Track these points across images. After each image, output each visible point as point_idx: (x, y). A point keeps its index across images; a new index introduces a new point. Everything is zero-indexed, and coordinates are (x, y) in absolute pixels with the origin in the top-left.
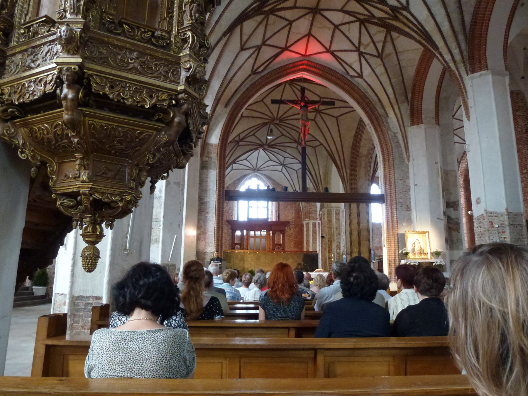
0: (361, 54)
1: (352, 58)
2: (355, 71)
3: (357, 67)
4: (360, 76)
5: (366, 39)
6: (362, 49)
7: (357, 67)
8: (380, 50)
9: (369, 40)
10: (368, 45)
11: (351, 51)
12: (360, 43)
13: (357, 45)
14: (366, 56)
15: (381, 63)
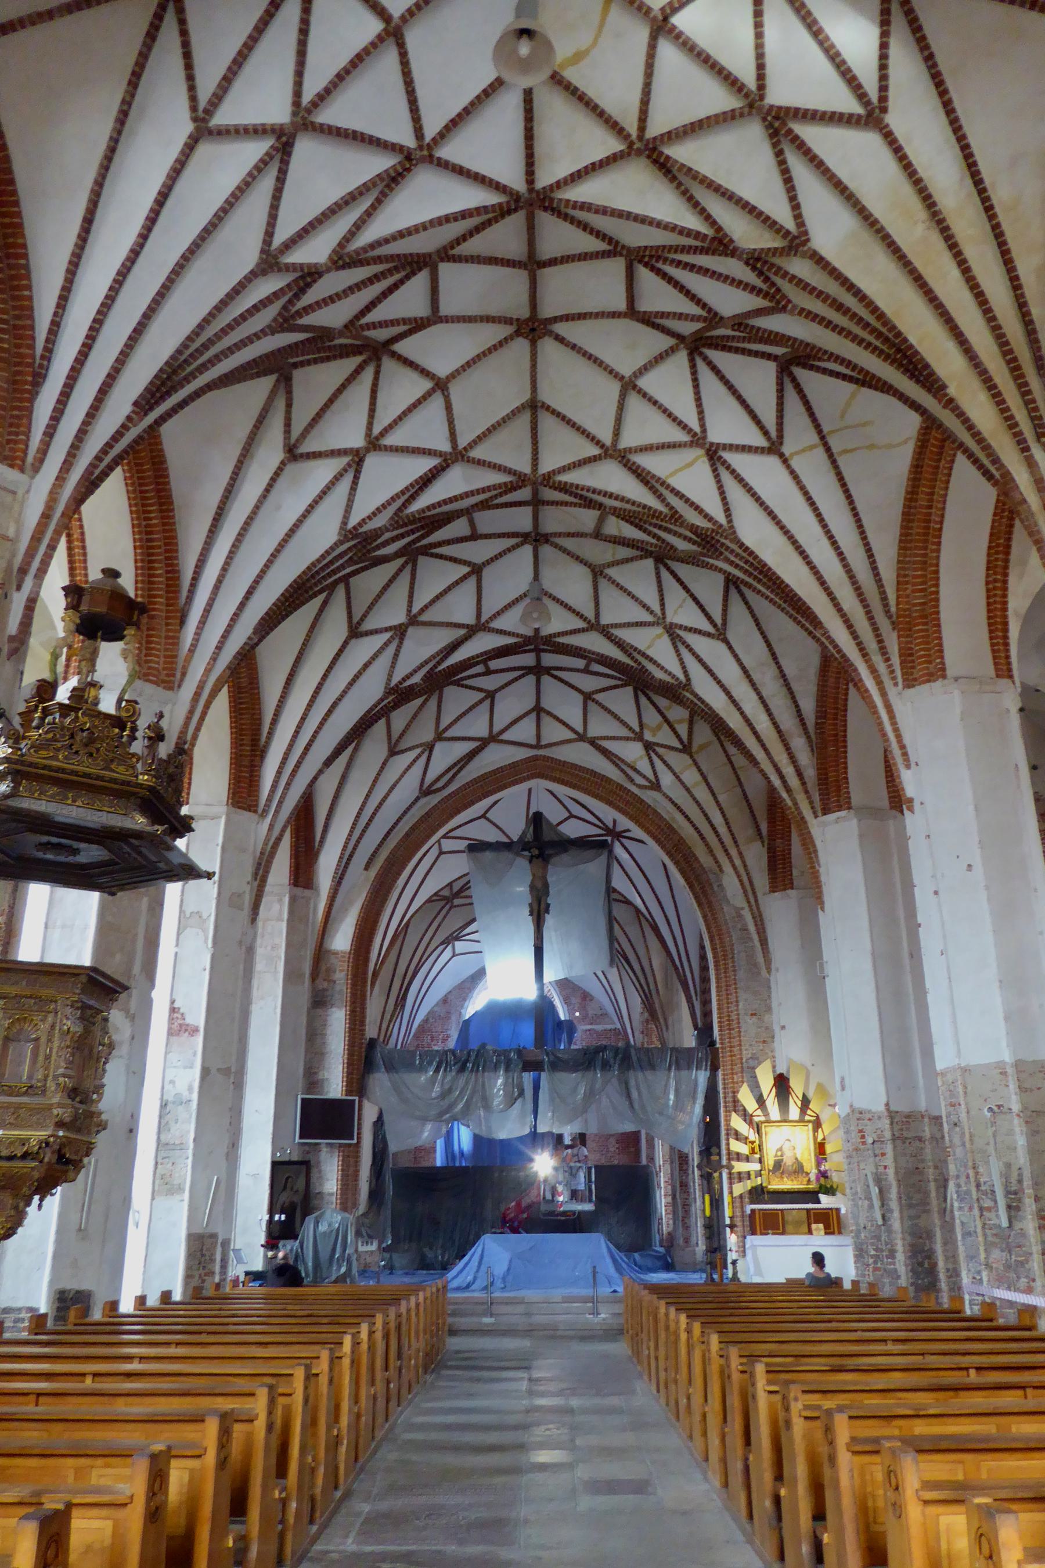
0: (649, 747)
1: (632, 752)
2: (644, 777)
3: (644, 766)
4: (656, 786)
5: (652, 717)
6: (648, 736)
7: (644, 766)
8: (685, 737)
9: (660, 718)
10: (659, 727)
11: (627, 739)
12: (641, 725)
13: (637, 729)
14: (661, 751)
15: (690, 762)
